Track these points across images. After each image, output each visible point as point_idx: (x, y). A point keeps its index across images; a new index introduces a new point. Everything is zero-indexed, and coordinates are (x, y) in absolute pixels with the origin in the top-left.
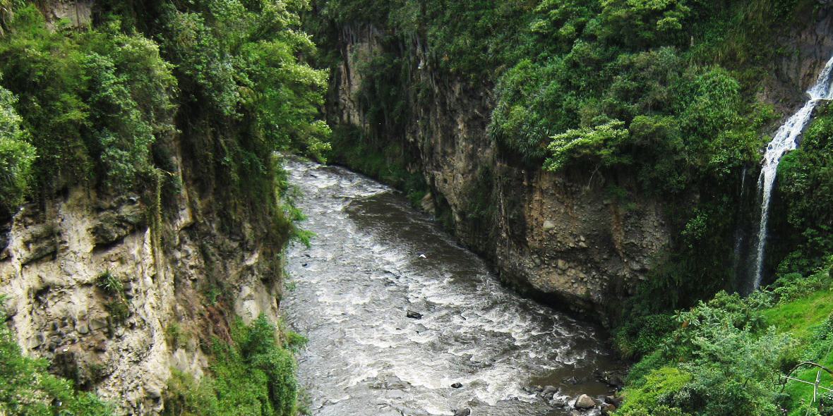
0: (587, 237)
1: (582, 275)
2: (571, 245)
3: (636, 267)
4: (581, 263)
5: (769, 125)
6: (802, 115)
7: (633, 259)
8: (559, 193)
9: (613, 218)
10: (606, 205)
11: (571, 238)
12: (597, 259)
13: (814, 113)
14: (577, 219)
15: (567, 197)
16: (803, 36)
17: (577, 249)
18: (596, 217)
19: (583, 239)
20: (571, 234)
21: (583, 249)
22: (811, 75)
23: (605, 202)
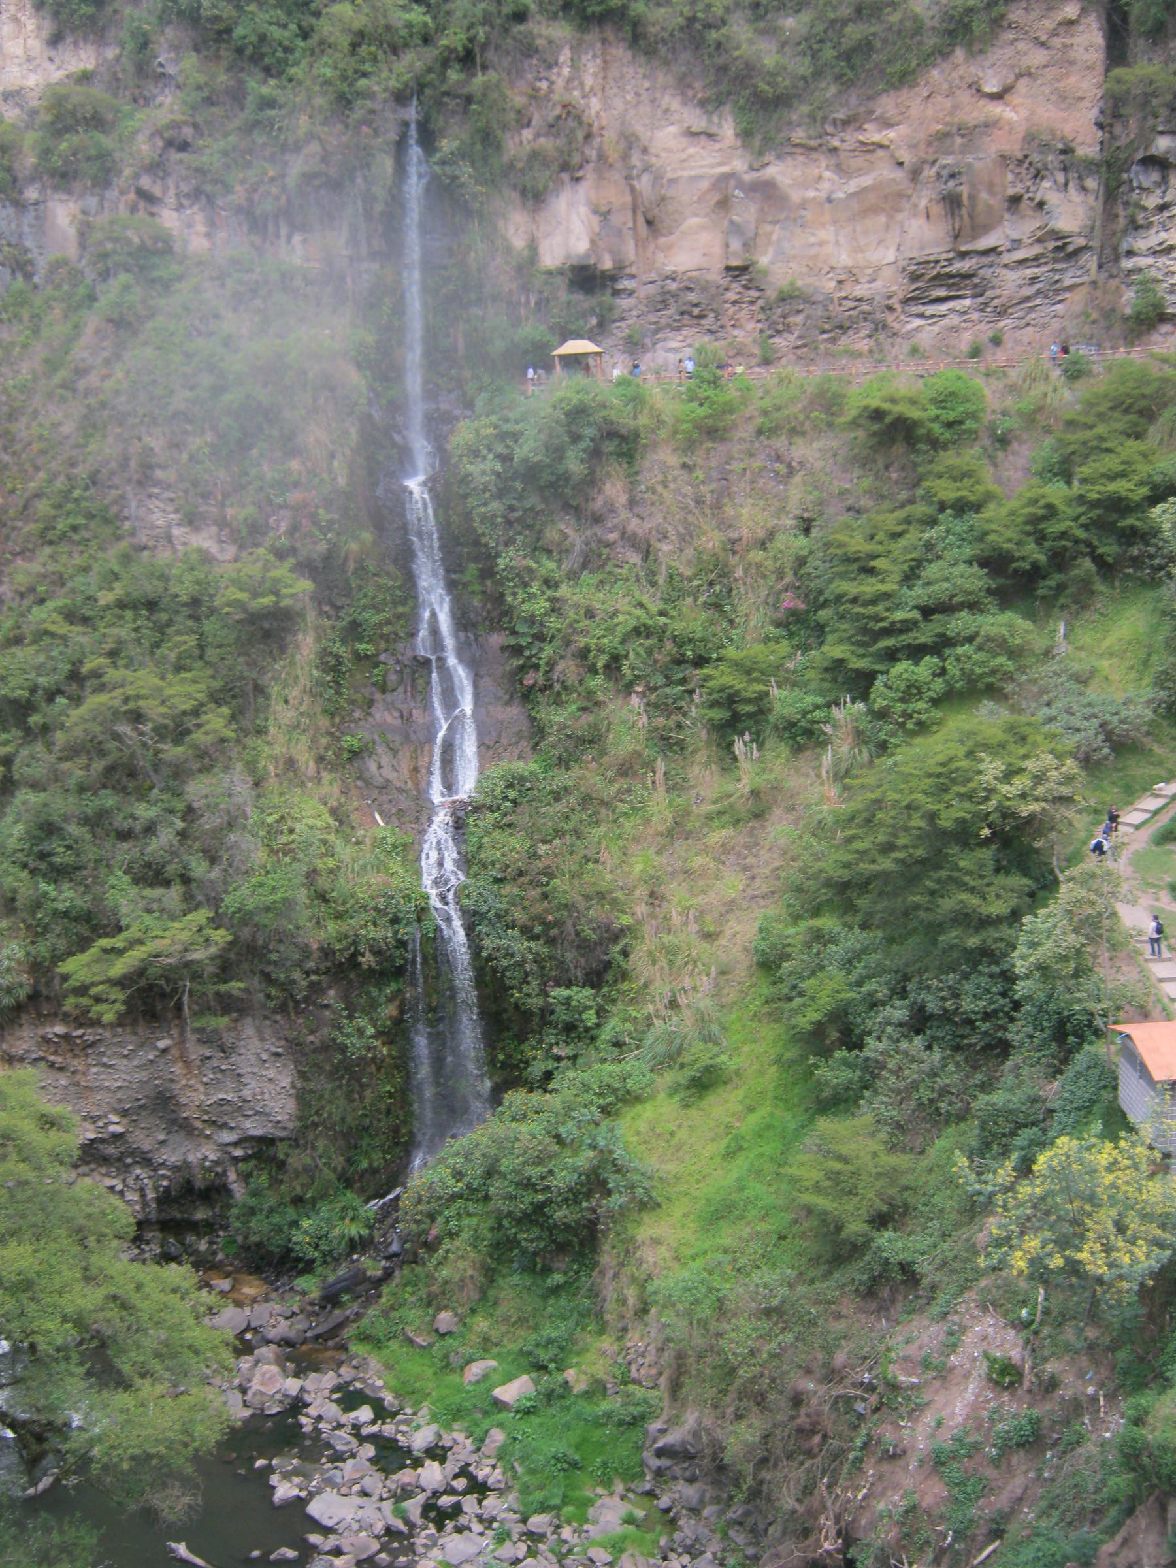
0: (124, 1113)
1: (109, 1182)
2: (92, 1136)
3: (227, 1137)
4: (105, 1160)
5: (409, 852)
6: (439, 827)
7: (225, 1126)
8: (55, 1053)
9: (177, 1069)
10: (165, 1051)
11: (88, 1125)
12: (146, 1145)
13: (459, 826)
14: (100, 1088)
15: (76, 1056)
16: (378, 716)
17: (102, 1141)
18: (143, 1075)
19: (115, 1119)
20: (85, 1118)
21: (117, 1137)
22: (416, 770)
23: (162, 1044)
